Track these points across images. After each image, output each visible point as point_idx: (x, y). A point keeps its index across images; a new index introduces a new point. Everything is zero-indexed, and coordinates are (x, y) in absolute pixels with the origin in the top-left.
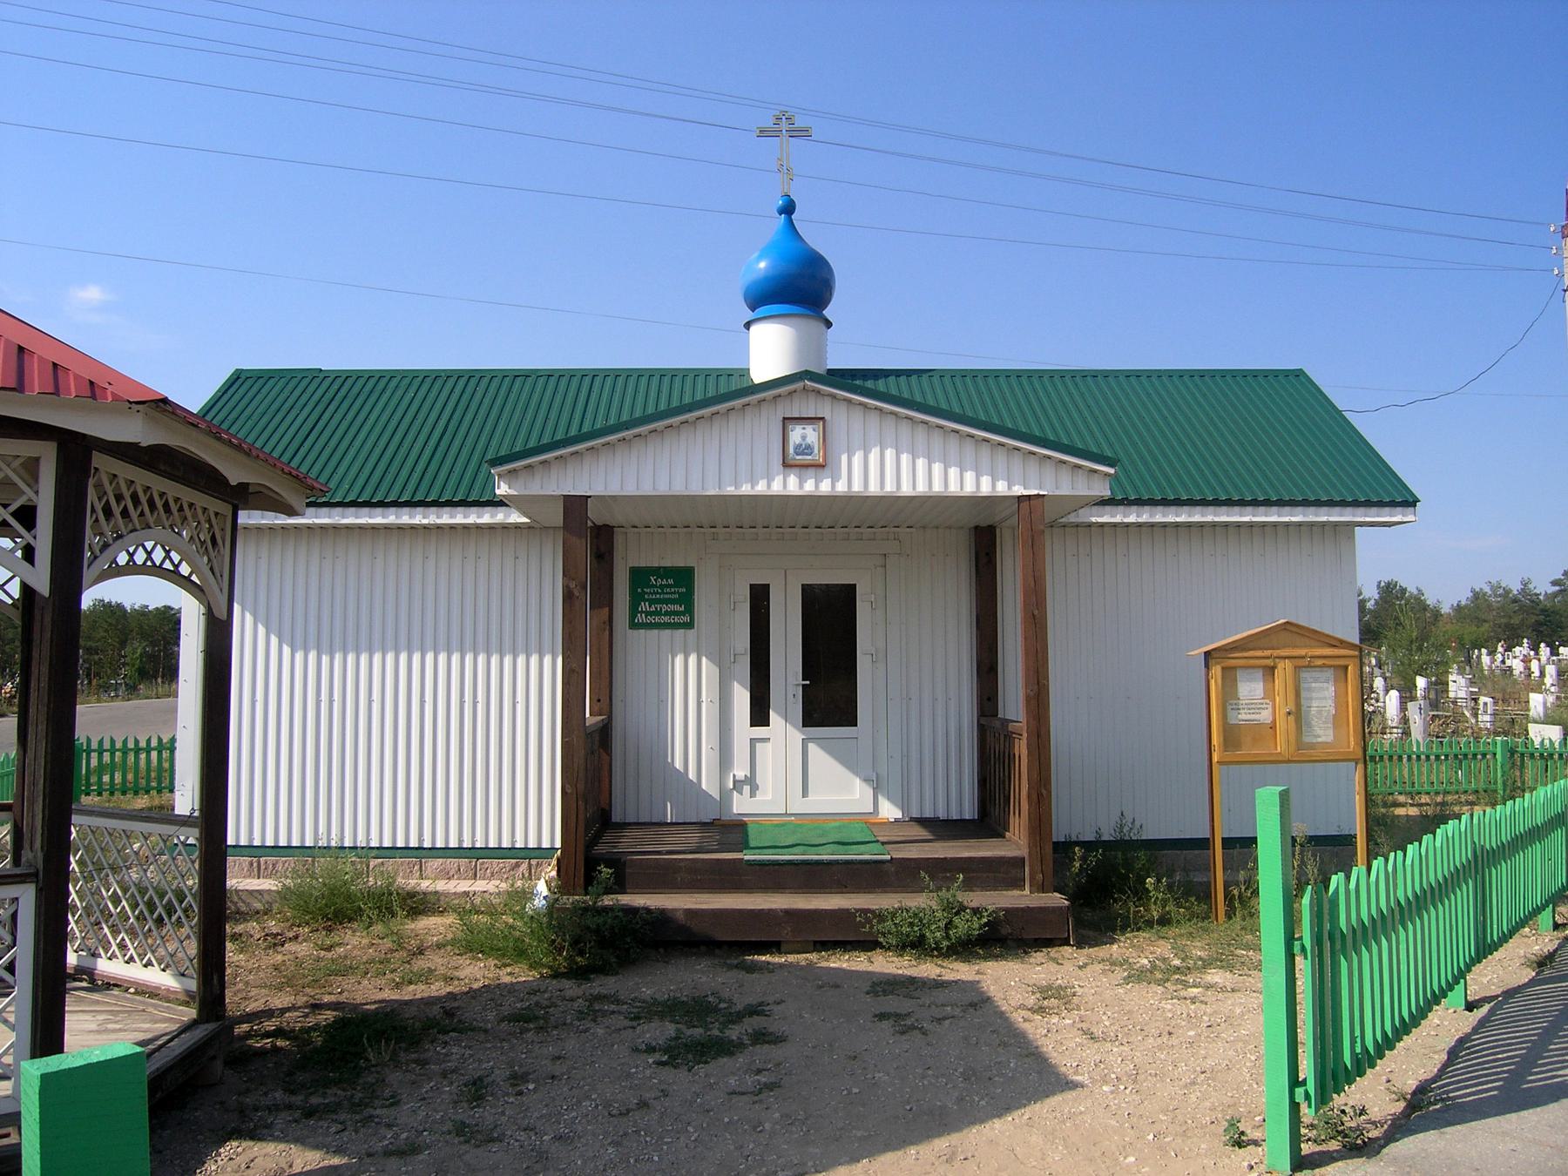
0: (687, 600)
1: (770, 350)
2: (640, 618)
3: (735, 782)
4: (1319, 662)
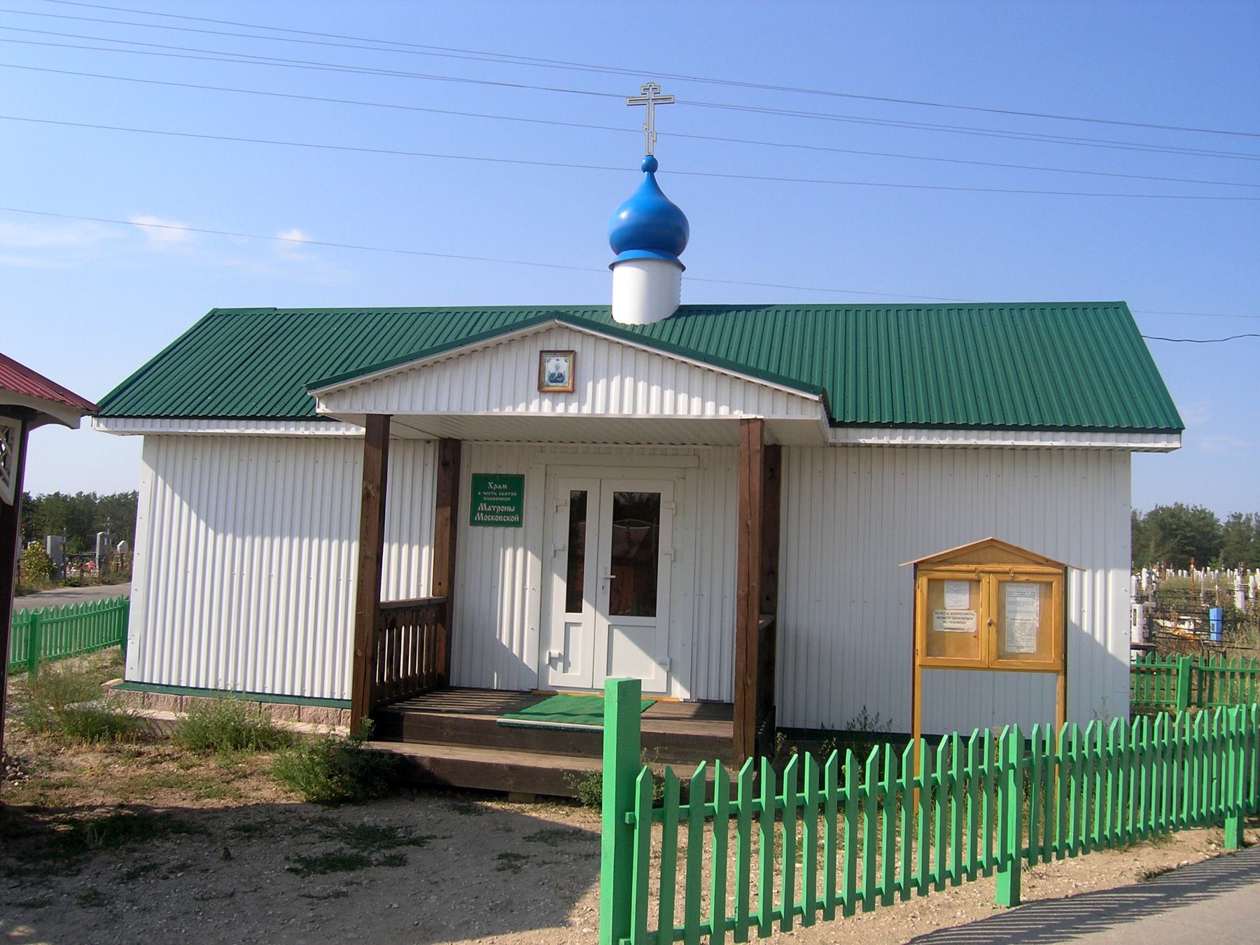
0: (518, 503)
1: (628, 293)
2: (479, 517)
3: (550, 659)
4: (1023, 578)
